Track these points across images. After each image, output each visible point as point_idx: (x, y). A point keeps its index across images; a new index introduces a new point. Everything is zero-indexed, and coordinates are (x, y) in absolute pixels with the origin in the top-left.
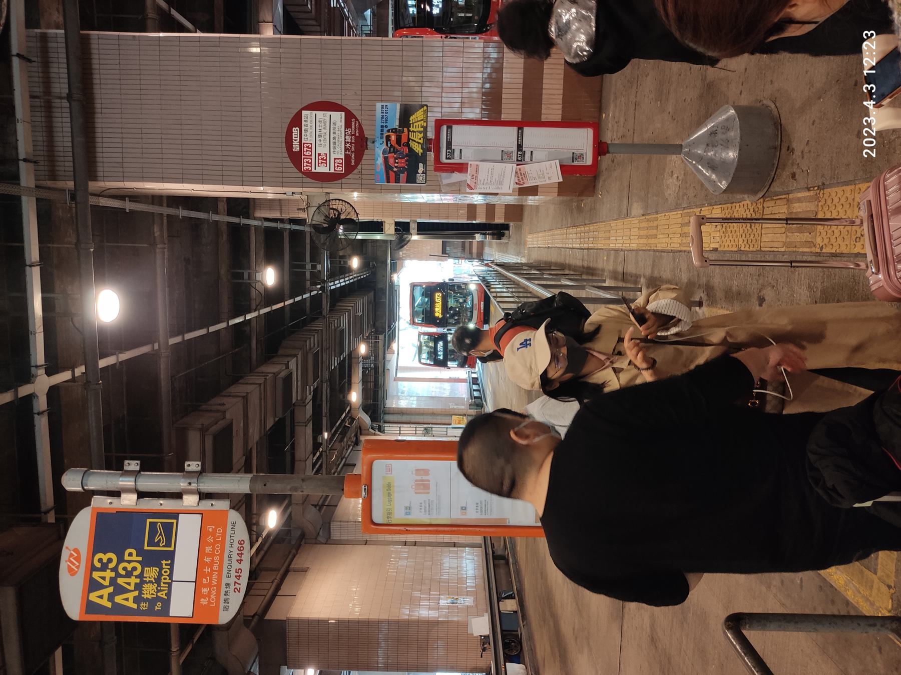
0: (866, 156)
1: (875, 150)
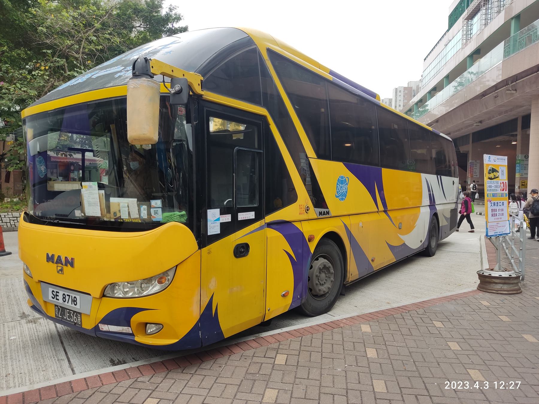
0: (445, 383)
1: (449, 388)
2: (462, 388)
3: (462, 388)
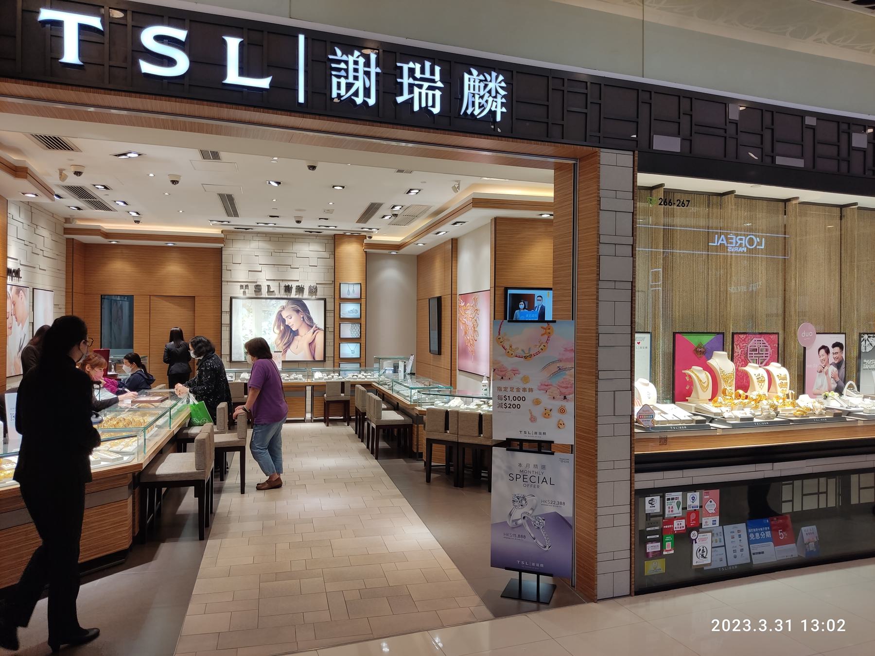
0: (713, 622)
1: (719, 630)
2: (740, 630)
3: (740, 630)
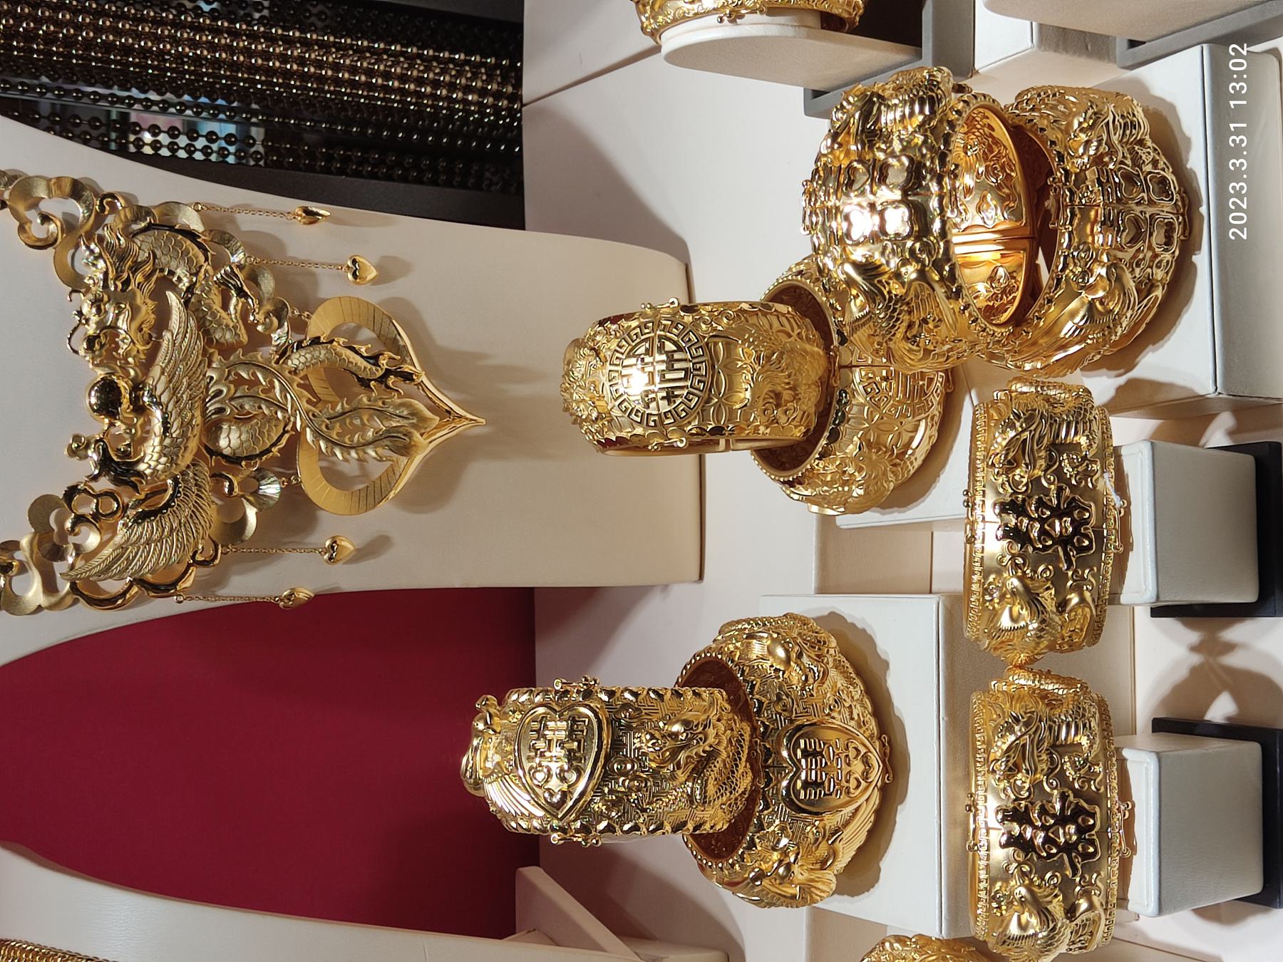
0: (1233, 238)
2: (1245, 199)
3: (1245, 199)
